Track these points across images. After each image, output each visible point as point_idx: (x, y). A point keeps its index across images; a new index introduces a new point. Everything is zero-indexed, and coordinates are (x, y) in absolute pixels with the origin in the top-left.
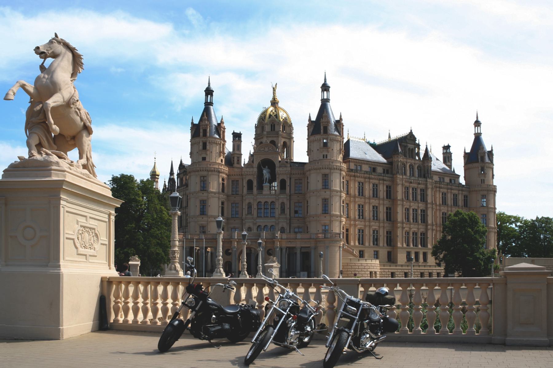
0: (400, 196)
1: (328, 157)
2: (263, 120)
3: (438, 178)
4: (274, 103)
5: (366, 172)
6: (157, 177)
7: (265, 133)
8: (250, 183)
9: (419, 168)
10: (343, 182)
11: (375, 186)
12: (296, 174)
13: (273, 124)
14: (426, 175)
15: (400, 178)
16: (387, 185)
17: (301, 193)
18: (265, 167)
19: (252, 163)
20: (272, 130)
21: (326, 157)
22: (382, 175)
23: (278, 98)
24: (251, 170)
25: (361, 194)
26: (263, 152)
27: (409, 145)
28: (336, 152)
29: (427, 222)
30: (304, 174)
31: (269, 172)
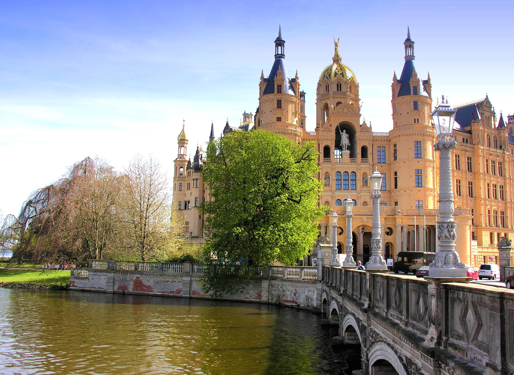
0: (482, 169)
2: (327, 78)
4: (337, 59)
6: (186, 142)
9: (495, 139)
11: (457, 156)
12: (379, 140)
13: (339, 84)
14: (503, 146)
15: (482, 149)
18: (342, 132)
19: (330, 127)
20: (338, 90)
21: (418, 122)
23: (341, 56)
24: (329, 133)
28: (427, 116)
29: (506, 199)
31: (347, 137)
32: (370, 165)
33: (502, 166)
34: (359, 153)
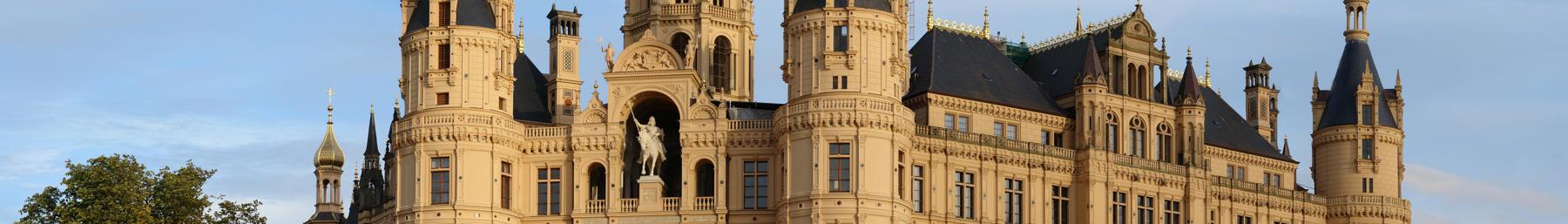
1: (851, 86)
3: (1226, 168)
5: (983, 140)
7: (657, 10)
8: (597, 175)
10: (901, 168)
11: (1015, 185)
12: (748, 142)
14: (1186, 156)
16: (1057, 183)
17: (765, 209)
18: (645, 121)
19: (603, 110)
21: (845, 86)
22: (1040, 149)
24: (601, 129)
25: (967, 212)
26: (638, 69)
27: (1128, 52)
30: (773, 141)
31: (660, 137)
32: (720, 216)
33: (1181, 213)
34: (685, 183)
